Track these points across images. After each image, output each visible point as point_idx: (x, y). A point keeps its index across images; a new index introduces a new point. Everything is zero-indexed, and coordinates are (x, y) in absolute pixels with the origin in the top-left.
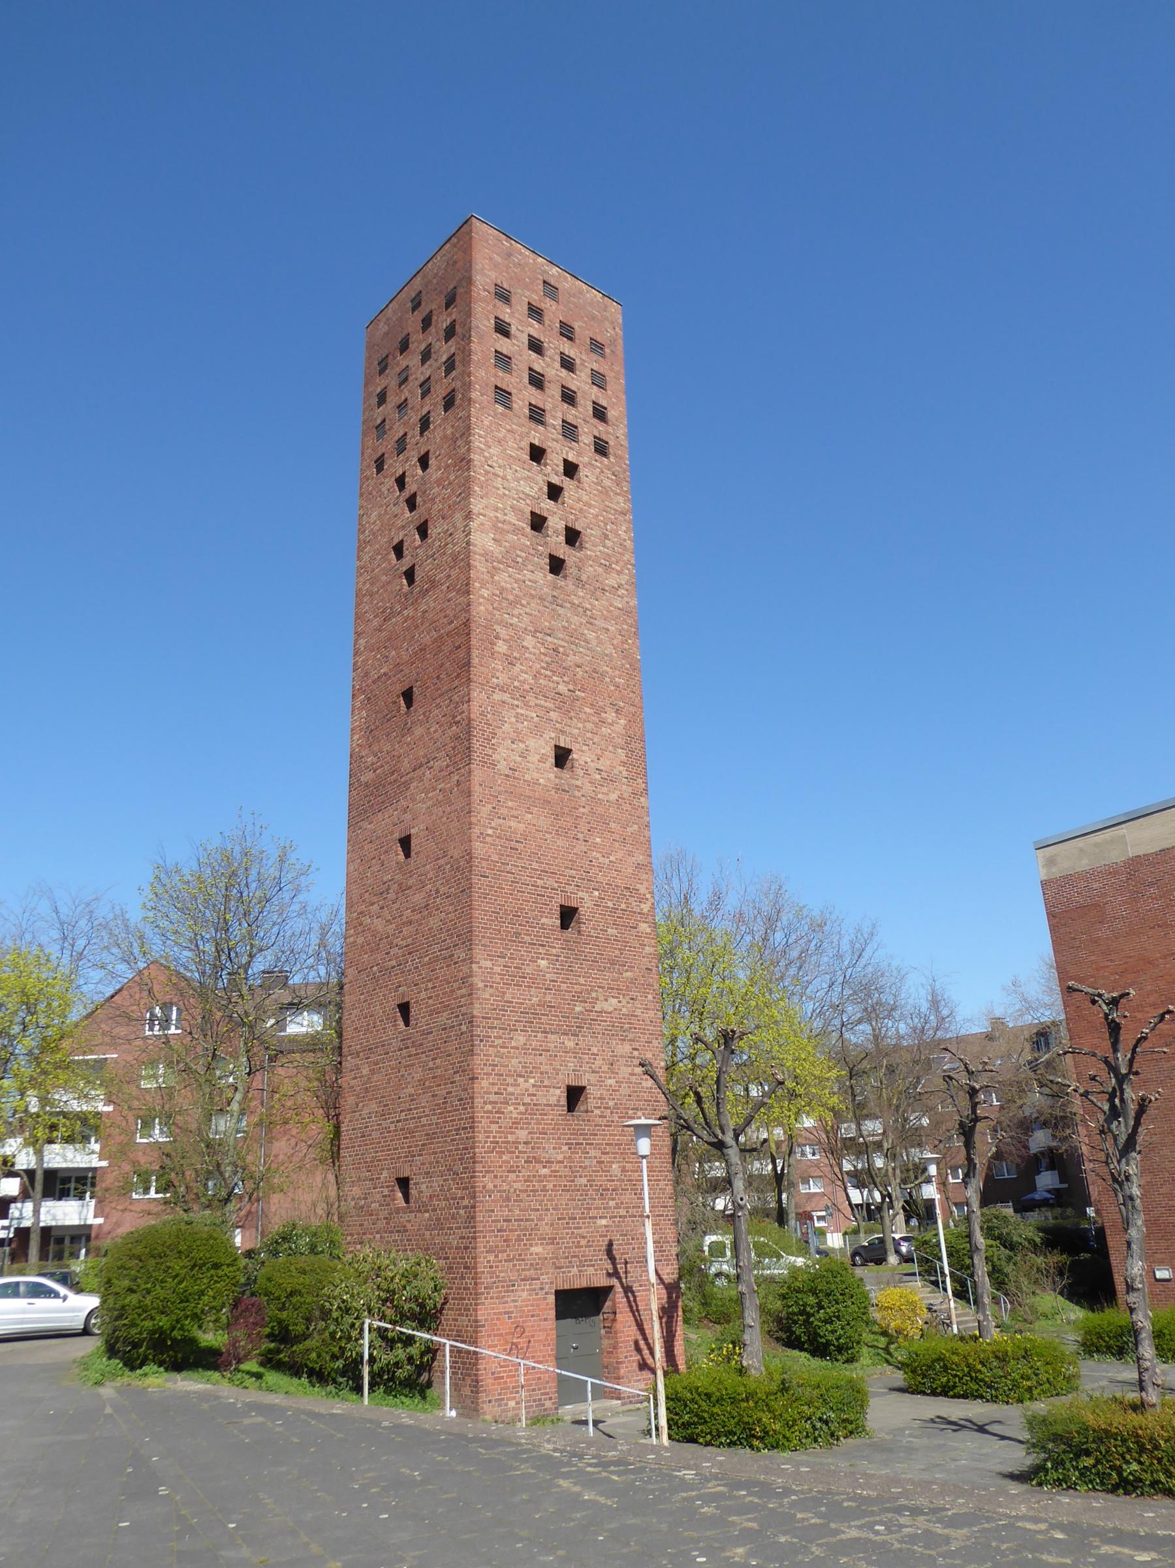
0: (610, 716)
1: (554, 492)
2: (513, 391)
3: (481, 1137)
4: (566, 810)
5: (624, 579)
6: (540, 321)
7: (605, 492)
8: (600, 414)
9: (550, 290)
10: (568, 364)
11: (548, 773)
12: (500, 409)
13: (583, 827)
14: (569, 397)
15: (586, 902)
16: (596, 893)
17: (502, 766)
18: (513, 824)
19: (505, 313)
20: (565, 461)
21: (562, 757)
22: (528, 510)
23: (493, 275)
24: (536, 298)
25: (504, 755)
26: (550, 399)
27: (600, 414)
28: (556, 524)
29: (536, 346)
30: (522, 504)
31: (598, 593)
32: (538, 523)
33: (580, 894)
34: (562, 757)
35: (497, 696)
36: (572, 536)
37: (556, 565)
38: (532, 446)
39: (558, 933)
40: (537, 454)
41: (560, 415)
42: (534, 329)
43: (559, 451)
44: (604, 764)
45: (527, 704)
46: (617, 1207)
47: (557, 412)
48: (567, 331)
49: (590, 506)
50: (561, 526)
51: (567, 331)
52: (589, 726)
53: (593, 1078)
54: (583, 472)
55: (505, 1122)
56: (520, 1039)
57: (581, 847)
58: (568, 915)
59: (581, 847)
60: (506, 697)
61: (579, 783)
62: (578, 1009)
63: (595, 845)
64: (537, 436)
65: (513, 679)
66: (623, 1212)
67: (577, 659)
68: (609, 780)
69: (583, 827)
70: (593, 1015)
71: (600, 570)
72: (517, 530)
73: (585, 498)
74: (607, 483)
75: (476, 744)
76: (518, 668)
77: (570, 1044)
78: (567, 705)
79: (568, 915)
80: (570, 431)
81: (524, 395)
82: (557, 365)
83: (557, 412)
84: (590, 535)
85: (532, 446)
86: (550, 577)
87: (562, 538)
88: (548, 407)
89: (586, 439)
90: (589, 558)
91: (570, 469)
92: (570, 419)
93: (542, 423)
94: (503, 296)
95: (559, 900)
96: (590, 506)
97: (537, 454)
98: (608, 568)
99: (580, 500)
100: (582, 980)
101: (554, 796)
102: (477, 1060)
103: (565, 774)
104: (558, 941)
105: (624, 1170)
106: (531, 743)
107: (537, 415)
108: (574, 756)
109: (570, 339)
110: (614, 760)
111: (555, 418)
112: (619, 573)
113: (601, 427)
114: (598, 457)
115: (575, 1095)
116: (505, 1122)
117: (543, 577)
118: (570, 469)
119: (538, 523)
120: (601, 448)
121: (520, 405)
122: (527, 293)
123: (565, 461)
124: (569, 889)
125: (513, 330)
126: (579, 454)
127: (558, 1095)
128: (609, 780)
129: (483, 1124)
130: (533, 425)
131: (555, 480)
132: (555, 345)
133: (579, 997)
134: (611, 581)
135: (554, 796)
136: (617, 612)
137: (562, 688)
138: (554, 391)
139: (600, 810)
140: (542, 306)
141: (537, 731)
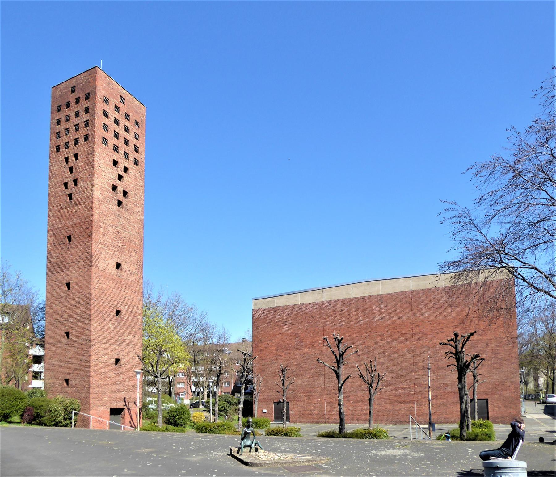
0: (133, 254)
1: (120, 177)
2: (109, 139)
3: (92, 370)
5: (140, 209)
6: (118, 112)
7: (136, 178)
8: (136, 149)
9: (122, 99)
10: (127, 130)
11: (114, 271)
12: (104, 146)
13: (124, 287)
14: (127, 143)
15: (123, 309)
17: (101, 268)
18: (104, 285)
19: (107, 108)
20: (124, 166)
21: (118, 266)
22: (112, 184)
23: (103, 92)
24: (118, 103)
25: (102, 264)
26: (120, 143)
27: (136, 149)
28: (120, 189)
29: (117, 122)
30: (110, 182)
32: (114, 188)
34: (118, 266)
35: (100, 246)
36: (125, 193)
37: (120, 203)
39: (115, 317)
40: (115, 163)
41: (123, 149)
43: (123, 163)
44: (131, 269)
45: (109, 249)
47: (123, 148)
48: (127, 117)
49: (131, 183)
50: (122, 190)
51: (127, 117)
52: (127, 257)
53: (123, 357)
54: (130, 171)
56: (103, 346)
57: (122, 293)
58: (118, 312)
59: (122, 293)
60: (103, 246)
64: (116, 157)
67: (125, 235)
68: (132, 274)
69: (124, 287)
71: (133, 206)
72: (108, 191)
73: (130, 180)
74: (137, 175)
75: (93, 260)
76: (107, 237)
77: (117, 348)
78: (121, 250)
79: (118, 312)
80: (126, 155)
81: (112, 141)
82: (123, 130)
83: (123, 148)
84: (131, 194)
87: (122, 194)
89: (131, 159)
90: (130, 202)
91: (126, 169)
94: (106, 101)
95: (116, 308)
96: (131, 183)
97: (115, 163)
98: (136, 205)
99: (128, 181)
101: (116, 278)
102: (91, 351)
103: (119, 271)
104: (115, 319)
106: (110, 261)
107: (116, 149)
108: (122, 266)
109: (128, 120)
110: (133, 268)
111: (122, 150)
113: (137, 154)
114: (135, 166)
115: (117, 361)
117: (115, 207)
118: (126, 169)
119: (114, 188)
120: (136, 163)
122: (115, 100)
123: (124, 166)
124: (119, 305)
125: (109, 115)
126: (129, 164)
127: (113, 361)
128: (132, 274)
129: (92, 367)
130: (114, 152)
131: (121, 173)
132: (123, 122)
133: (120, 335)
135: (116, 278)
136: (138, 221)
137: (120, 244)
138: (122, 140)
139: (129, 283)
141: (112, 258)
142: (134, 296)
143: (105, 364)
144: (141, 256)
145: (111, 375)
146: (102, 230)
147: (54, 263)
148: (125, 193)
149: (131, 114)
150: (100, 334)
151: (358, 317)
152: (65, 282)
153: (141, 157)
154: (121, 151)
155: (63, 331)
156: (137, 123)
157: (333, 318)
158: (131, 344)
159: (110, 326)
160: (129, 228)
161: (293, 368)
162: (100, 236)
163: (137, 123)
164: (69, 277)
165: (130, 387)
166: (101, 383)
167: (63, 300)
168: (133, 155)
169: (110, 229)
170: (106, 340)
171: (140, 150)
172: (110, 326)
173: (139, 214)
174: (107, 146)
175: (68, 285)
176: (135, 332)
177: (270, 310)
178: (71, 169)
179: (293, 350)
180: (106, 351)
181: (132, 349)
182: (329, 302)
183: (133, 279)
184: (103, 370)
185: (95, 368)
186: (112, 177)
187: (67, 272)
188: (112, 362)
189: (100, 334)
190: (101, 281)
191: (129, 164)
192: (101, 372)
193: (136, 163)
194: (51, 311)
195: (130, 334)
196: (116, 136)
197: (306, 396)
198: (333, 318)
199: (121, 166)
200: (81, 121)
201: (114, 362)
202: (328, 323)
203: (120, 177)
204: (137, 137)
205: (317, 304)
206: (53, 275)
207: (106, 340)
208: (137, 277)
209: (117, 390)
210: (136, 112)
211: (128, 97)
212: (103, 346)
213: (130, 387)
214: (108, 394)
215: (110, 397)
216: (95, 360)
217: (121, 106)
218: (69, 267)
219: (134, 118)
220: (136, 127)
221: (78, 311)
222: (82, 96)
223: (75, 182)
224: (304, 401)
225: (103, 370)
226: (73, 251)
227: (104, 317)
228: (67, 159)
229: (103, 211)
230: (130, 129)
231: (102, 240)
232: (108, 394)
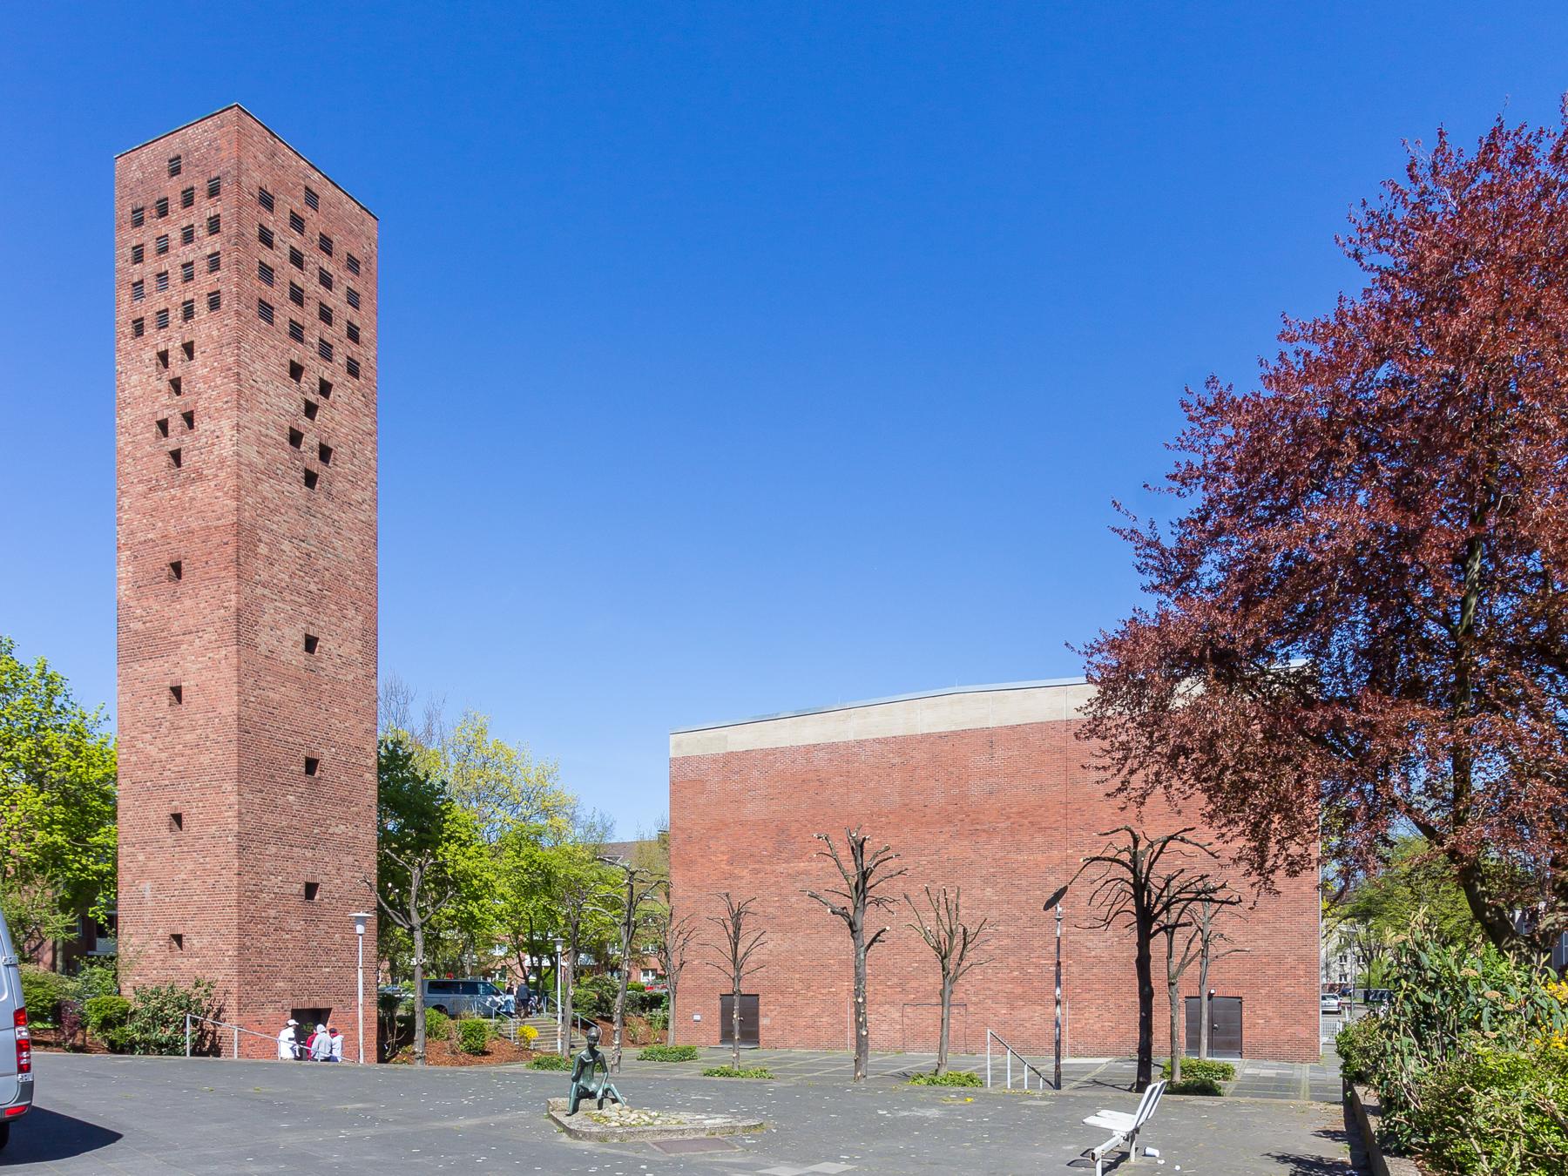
0: (351, 613)
1: (310, 410)
2: (276, 306)
5: (368, 495)
6: (301, 232)
7: (354, 412)
8: (353, 333)
9: (312, 198)
10: (326, 281)
11: (298, 656)
12: (264, 323)
13: (326, 700)
14: (326, 315)
15: (325, 755)
17: (263, 649)
18: (271, 694)
19: (270, 221)
20: (321, 380)
21: (311, 644)
22: (287, 426)
23: (257, 176)
24: (299, 205)
26: (308, 317)
27: (353, 333)
28: (310, 440)
29: (297, 259)
30: (282, 421)
31: (345, 507)
32: (295, 438)
34: (311, 644)
35: (259, 591)
36: (325, 453)
37: (310, 479)
38: (292, 362)
40: (296, 371)
41: (317, 333)
42: (296, 240)
43: (316, 369)
44: (343, 651)
45: (283, 600)
47: (315, 331)
48: (326, 245)
49: (342, 425)
50: (315, 443)
51: (326, 245)
52: (334, 620)
53: (325, 878)
55: (260, 904)
56: (272, 849)
57: (323, 715)
58: (311, 765)
60: (266, 592)
64: (297, 353)
65: (272, 577)
68: (348, 664)
71: (348, 486)
72: (277, 444)
73: (337, 418)
74: (357, 404)
77: (309, 854)
78: (315, 602)
79: (311, 765)
80: (326, 351)
81: (286, 311)
82: (316, 280)
83: (315, 331)
84: (341, 453)
85: (292, 362)
86: (306, 489)
87: (316, 454)
88: (307, 324)
89: (340, 359)
90: (338, 474)
91: (325, 388)
92: (327, 338)
93: (302, 341)
94: (267, 201)
95: (305, 753)
96: (342, 425)
97: (296, 371)
101: (304, 675)
106: (286, 631)
107: (296, 332)
109: (330, 254)
110: (352, 649)
111: (313, 336)
112: (364, 489)
113: (354, 347)
114: (350, 378)
115: (311, 890)
116: (260, 904)
117: (299, 491)
118: (325, 388)
119: (295, 438)
120: (353, 369)
121: (281, 320)
122: (290, 200)
123: (321, 380)
125: (276, 239)
126: (333, 374)
127: (299, 888)
128: (348, 664)
130: (293, 342)
131: (312, 398)
132: (315, 259)
133: (316, 823)
134: (357, 496)
135: (304, 675)
136: (360, 525)
137: (313, 587)
138: (312, 308)
139: (339, 687)
140: (304, 215)
144: (372, 618)
145: (295, 924)
146: (263, 549)
147: (136, 632)
148: (325, 453)
149: (334, 238)
151: (932, 783)
152: (168, 684)
153: (366, 354)
154: (312, 338)
155: (165, 813)
156: (353, 264)
157: (872, 785)
158: (348, 846)
160: (338, 544)
161: (770, 910)
162: (260, 564)
163: (353, 264)
164: (178, 671)
165: (345, 954)
167: (163, 730)
168: (342, 350)
169: (286, 546)
170: (280, 835)
171: (363, 335)
173: (365, 506)
174: (271, 323)
175: (177, 692)
176: (358, 814)
178: (176, 385)
179: (770, 863)
181: (350, 859)
182: (861, 743)
183: (350, 678)
184: (272, 913)
185: (252, 907)
186: (287, 406)
187: (173, 658)
190: (264, 684)
191: (335, 372)
193: (353, 369)
194: (134, 759)
195: (344, 819)
196: (297, 296)
198: (872, 785)
199: (310, 381)
200: (200, 254)
202: (860, 797)
203: (310, 410)
204: (353, 299)
205: (832, 748)
206: (136, 666)
207: (280, 835)
210: (351, 232)
211: (327, 192)
212: (272, 849)
213: (345, 954)
214: (285, 971)
215: (291, 980)
217: (308, 214)
218: (178, 645)
219: (346, 249)
220: (351, 274)
221: (205, 759)
222: (200, 185)
223: (189, 418)
225: (272, 913)
226: (188, 603)
227: (272, 776)
228: (163, 357)
229: (265, 499)
230: (335, 278)
231: (264, 576)
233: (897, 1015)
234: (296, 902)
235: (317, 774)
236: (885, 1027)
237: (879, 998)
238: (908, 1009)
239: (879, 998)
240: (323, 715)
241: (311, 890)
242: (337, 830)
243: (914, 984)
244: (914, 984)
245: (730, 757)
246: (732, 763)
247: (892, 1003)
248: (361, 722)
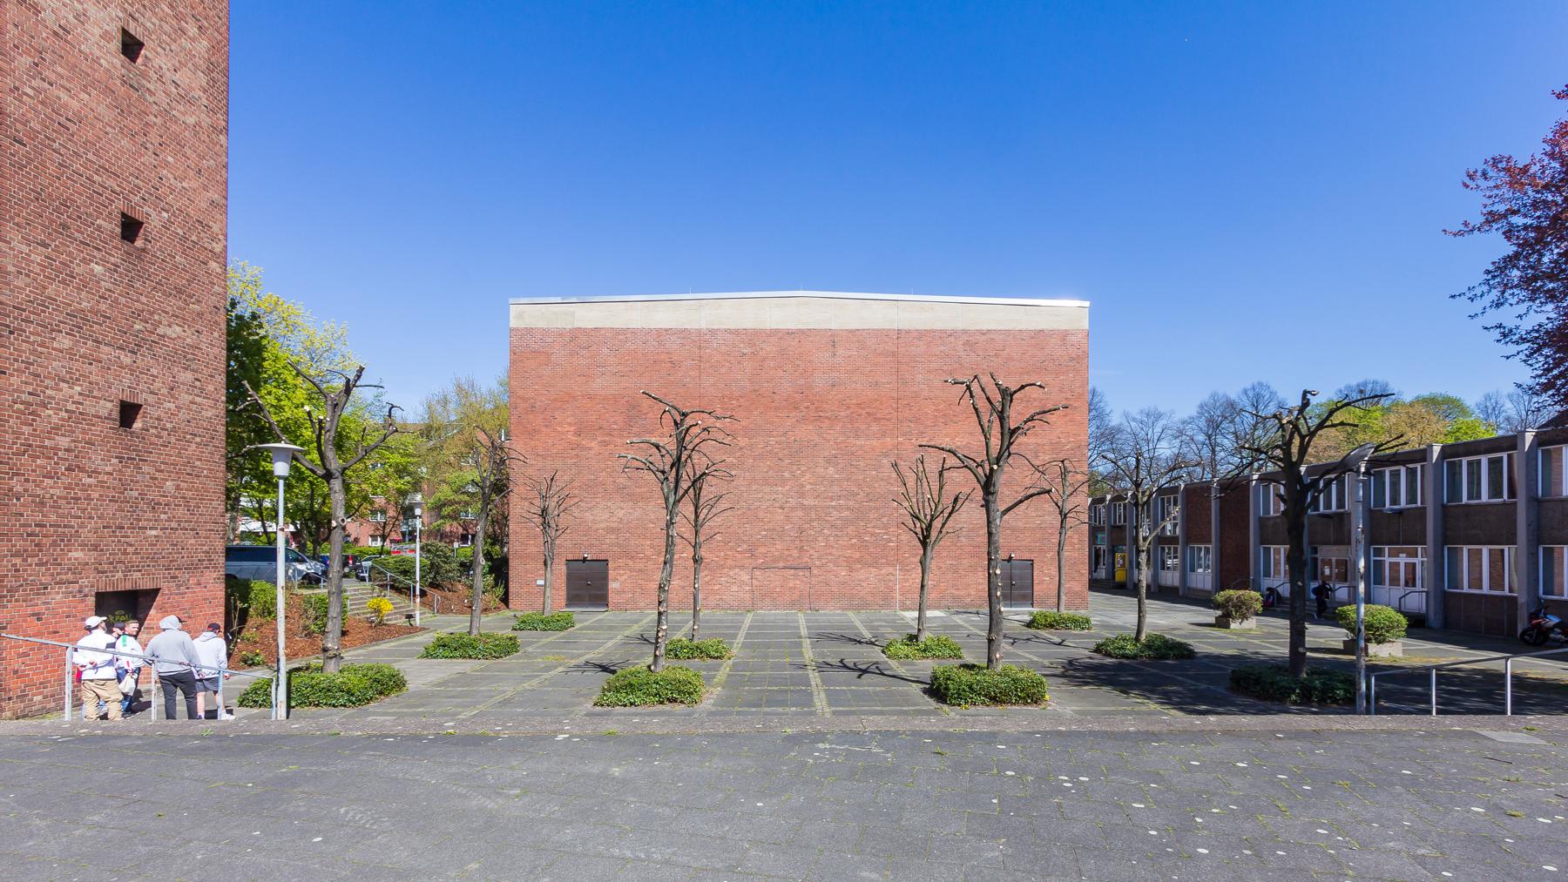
0: (192, 30)
4: (135, 111)
15: (154, 220)
16: (165, 215)
33: (146, 209)
46: (169, 520)
53: (151, 399)
58: (131, 228)
59: (148, 159)
61: (152, 88)
62: (137, 327)
63: (167, 164)
66: (174, 525)
70: (154, 337)
77: (126, 359)
79: (131, 228)
95: (120, 205)
100: (143, 299)
105: (178, 488)
115: (128, 412)
133: (137, 315)
142: (194, 184)
143: (78, 417)
145: (100, 460)
150: (50, 291)
159: (98, 269)
165: (181, 512)
166: (57, 492)
170: (79, 323)
172: (98, 269)
176: (200, 315)
177: (561, 334)
180: (76, 365)
183: (191, 120)
184: (64, 442)
188: (104, 413)
189: (50, 291)
192: (56, 449)
197: (652, 546)
201: (116, 415)
207: (79, 323)
208: (206, 121)
209: (126, 524)
212: (65, 342)
213: (181, 512)
214: (86, 535)
215: (95, 547)
216: (24, 397)
224: (648, 559)
225: (64, 442)
227: (65, 226)
232: (86, 535)
233: (746, 578)
234: (107, 428)
235: (139, 243)
236: (735, 588)
237: (730, 562)
238: (757, 573)
239: (730, 562)
240: (148, 159)
241: (128, 412)
242: (169, 332)
243: (762, 550)
244: (762, 550)
245: (576, 334)
246: (578, 339)
247: (742, 567)
248: (205, 188)
